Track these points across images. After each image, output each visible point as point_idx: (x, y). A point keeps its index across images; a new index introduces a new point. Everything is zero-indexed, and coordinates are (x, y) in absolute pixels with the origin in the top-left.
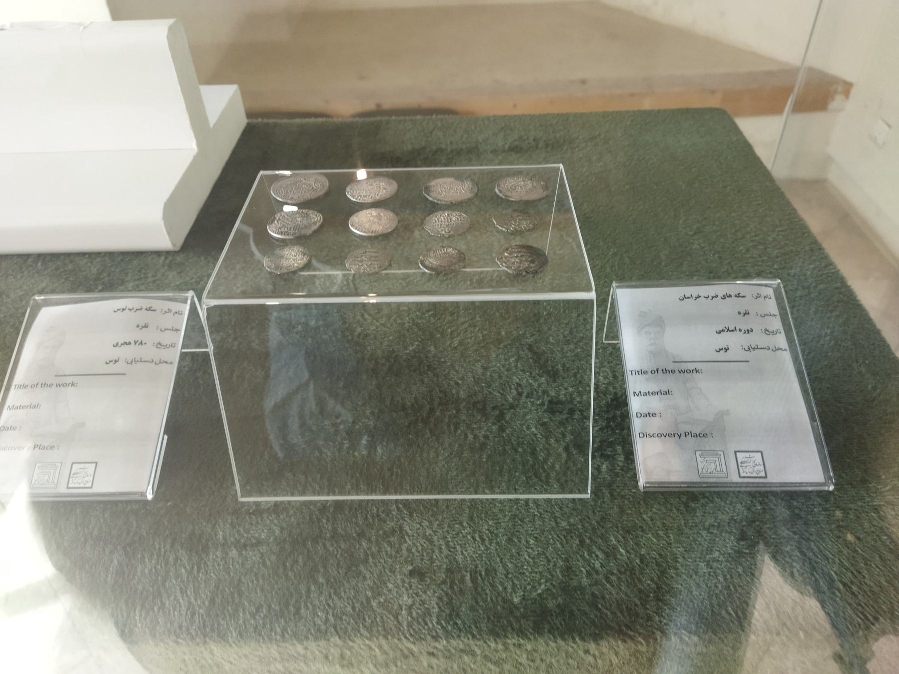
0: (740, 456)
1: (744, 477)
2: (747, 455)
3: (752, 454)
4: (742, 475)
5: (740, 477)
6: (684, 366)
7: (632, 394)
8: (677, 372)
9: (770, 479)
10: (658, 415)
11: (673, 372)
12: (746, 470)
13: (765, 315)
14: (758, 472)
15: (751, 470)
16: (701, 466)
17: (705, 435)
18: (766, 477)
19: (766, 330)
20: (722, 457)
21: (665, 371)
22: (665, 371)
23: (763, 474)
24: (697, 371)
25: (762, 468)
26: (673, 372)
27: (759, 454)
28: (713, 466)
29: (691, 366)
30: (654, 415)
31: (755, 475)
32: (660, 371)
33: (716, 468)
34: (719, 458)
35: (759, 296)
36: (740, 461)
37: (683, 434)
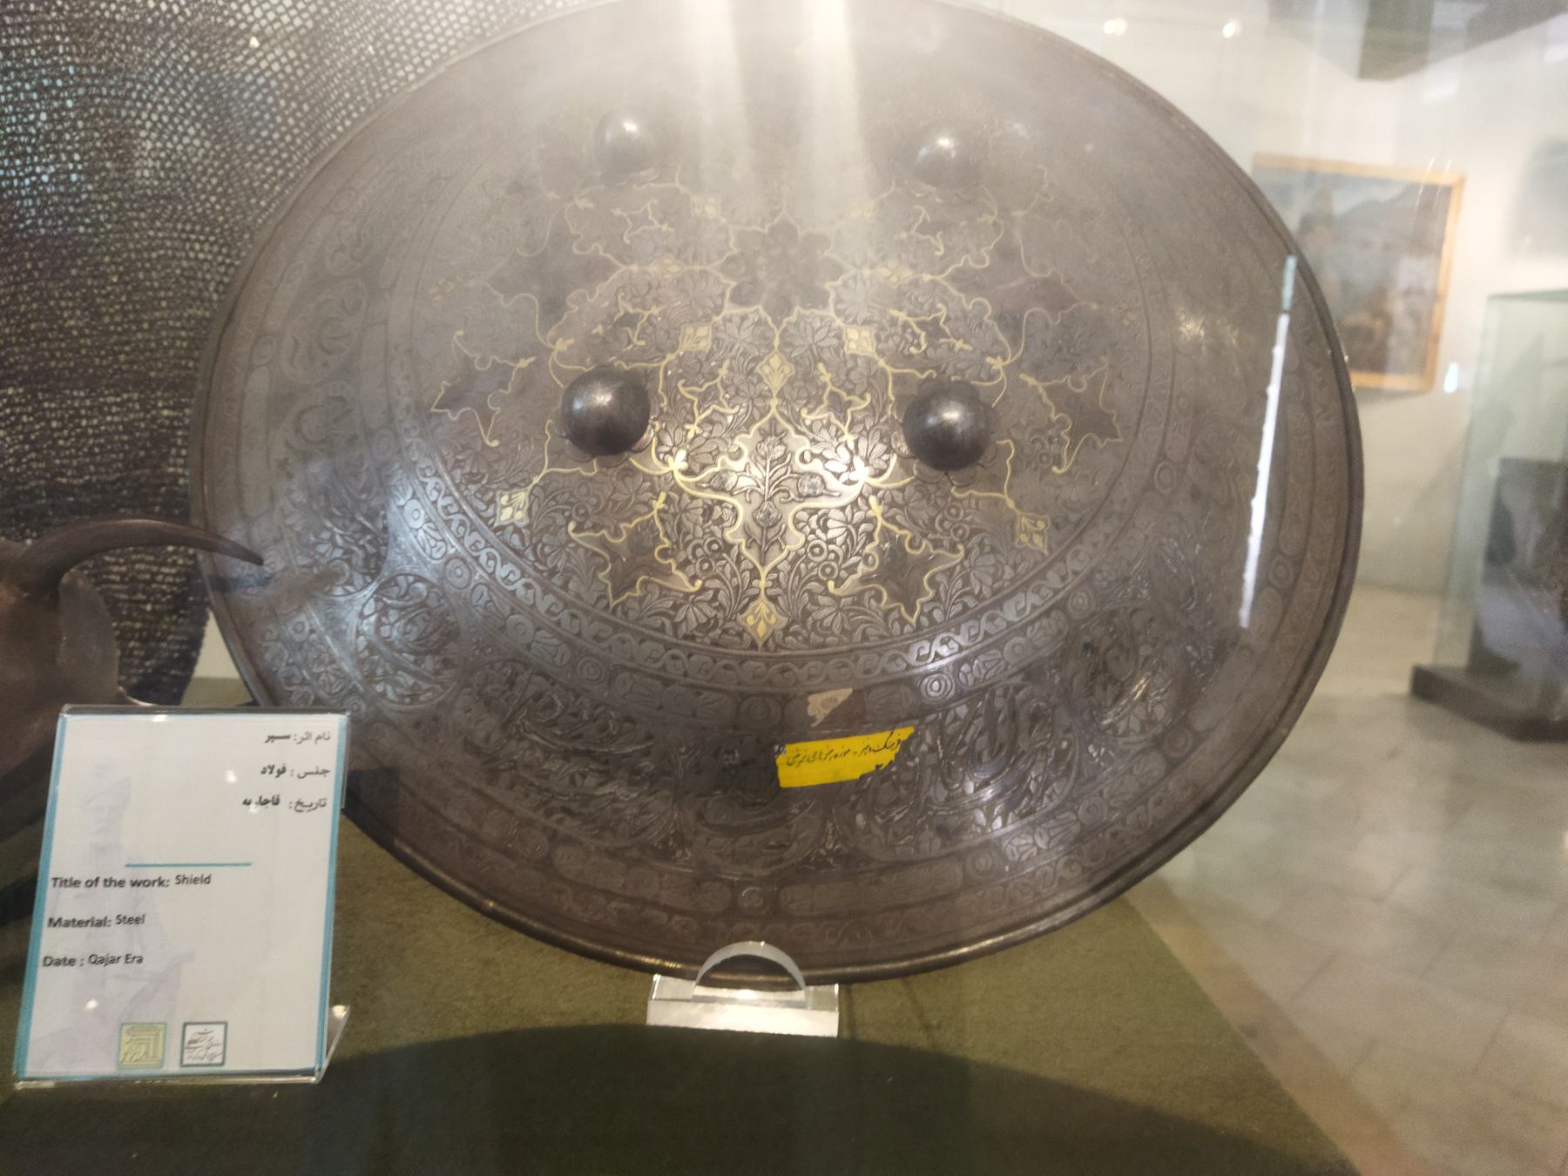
2: (201, 1028)
3: (210, 1028)
5: (182, 1065)
6: (142, 875)
7: (46, 922)
8: (128, 885)
9: (229, 1067)
10: (78, 963)
11: (121, 883)
14: (214, 1056)
16: (125, 1048)
18: (222, 1064)
19: (299, 803)
21: (109, 882)
22: (109, 882)
23: (218, 1060)
25: (220, 1049)
26: (121, 883)
27: (222, 1027)
28: (143, 1049)
29: (152, 874)
30: (72, 962)
31: (205, 1061)
32: (101, 883)
35: (308, 736)
36: (188, 1038)
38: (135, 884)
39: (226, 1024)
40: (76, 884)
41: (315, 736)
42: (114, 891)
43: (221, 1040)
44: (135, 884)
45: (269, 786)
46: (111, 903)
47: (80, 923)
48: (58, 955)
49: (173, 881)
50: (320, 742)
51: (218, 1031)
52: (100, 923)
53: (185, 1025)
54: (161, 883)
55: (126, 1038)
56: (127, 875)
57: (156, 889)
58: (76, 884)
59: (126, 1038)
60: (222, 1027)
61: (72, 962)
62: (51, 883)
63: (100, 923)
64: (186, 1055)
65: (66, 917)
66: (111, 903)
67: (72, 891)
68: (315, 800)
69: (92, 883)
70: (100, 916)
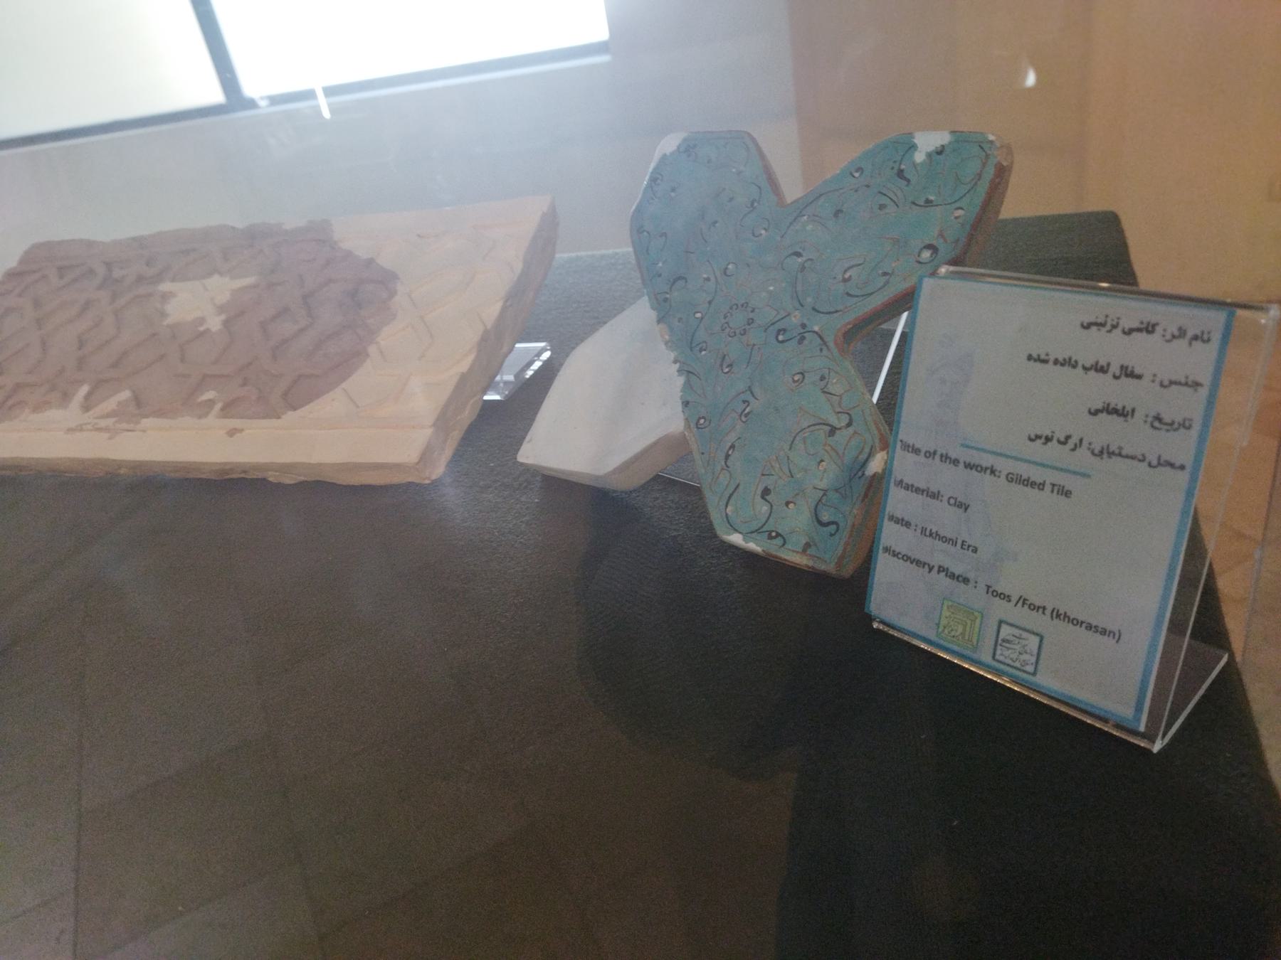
0: (1006, 631)
1: (999, 661)
2: (1017, 632)
3: (1025, 635)
4: (997, 657)
8: (961, 465)
11: (955, 462)
12: (1007, 653)
13: (1172, 383)
14: (1025, 663)
15: (1014, 656)
16: (944, 622)
17: (966, 581)
18: (1034, 674)
19: (1158, 418)
20: (978, 621)
21: (945, 458)
22: (945, 458)
23: (1030, 669)
24: (993, 472)
25: (1033, 660)
26: (955, 462)
27: (1037, 639)
28: (960, 629)
29: (987, 460)
30: (908, 525)
31: (1017, 664)
32: (937, 457)
33: (963, 634)
34: (973, 621)
35: (1182, 333)
37: (936, 569)
38: (969, 466)
40: (916, 451)
41: (1190, 334)
42: (947, 467)
43: (1035, 652)
44: (969, 466)
46: (948, 479)
47: (918, 490)
48: (899, 515)
50: (1198, 345)
51: (1034, 641)
52: (935, 496)
54: (993, 472)
55: (946, 613)
57: (988, 477)
58: (916, 451)
59: (946, 613)
61: (908, 525)
63: (935, 496)
64: (998, 652)
66: (948, 479)
67: (911, 457)
68: (1179, 419)
69: (931, 454)
70: (934, 489)
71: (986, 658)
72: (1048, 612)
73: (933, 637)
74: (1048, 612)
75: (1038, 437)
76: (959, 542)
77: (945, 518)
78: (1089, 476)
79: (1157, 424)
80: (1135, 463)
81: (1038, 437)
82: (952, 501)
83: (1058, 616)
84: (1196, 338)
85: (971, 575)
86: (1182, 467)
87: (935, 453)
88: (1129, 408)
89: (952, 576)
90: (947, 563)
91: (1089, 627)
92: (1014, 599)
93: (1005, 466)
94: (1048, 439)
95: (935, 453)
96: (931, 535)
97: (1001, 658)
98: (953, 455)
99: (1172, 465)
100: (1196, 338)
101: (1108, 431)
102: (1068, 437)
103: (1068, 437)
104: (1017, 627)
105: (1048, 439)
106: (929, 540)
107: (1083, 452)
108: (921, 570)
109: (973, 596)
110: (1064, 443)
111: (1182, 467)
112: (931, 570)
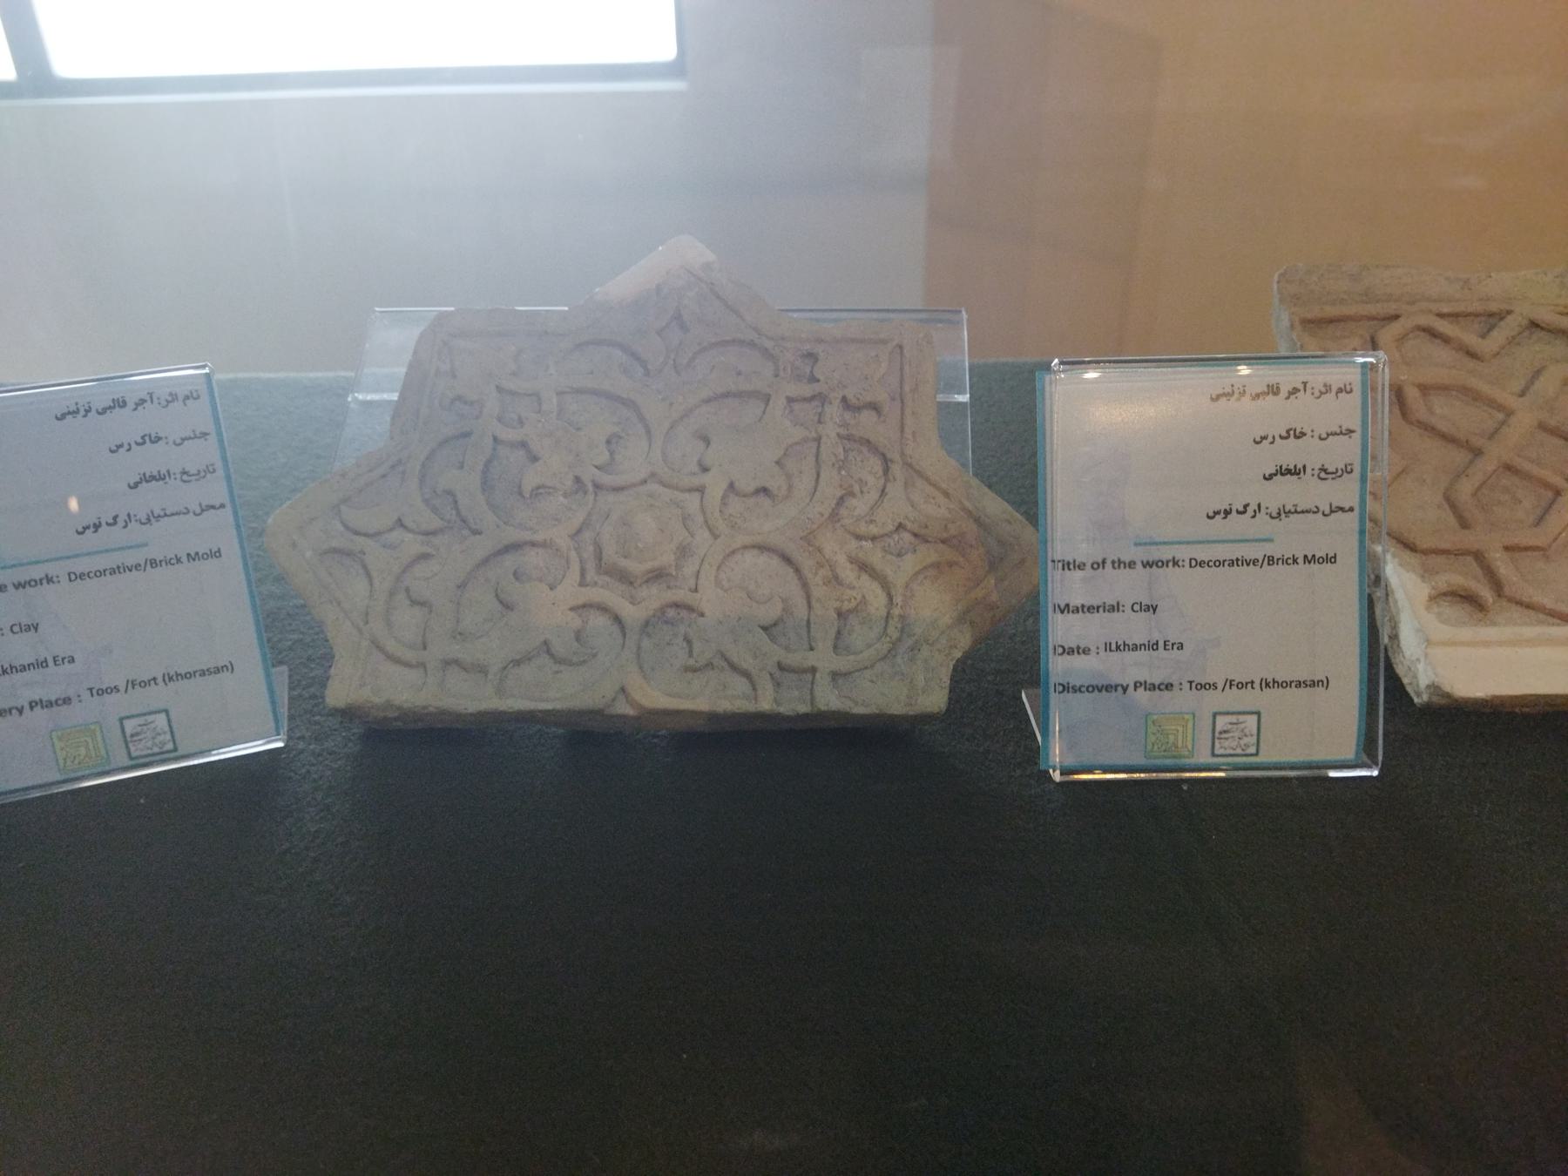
0: (1222, 722)
2: (1233, 719)
3: (1242, 718)
5: (1213, 755)
8: (1139, 566)
11: (1132, 565)
12: (1226, 744)
14: (1247, 746)
15: (1234, 744)
17: (1169, 687)
20: (1190, 725)
23: (1252, 750)
24: (1175, 563)
25: (1254, 740)
26: (1132, 565)
27: (1255, 717)
29: (1166, 553)
31: (1239, 751)
32: (1108, 565)
36: (1218, 728)
39: (1258, 714)
40: (1081, 567)
41: (1334, 389)
43: (1255, 731)
45: (1289, 453)
46: (1126, 586)
47: (1091, 609)
49: (1187, 563)
51: (1251, 721)
52: (1115, 608)
53: (1215, 715)
54: (1175, 563)
56: (1139, 554)
60: (1255, 717)
62: (1050, 564)
63: (1115, 608)
64: (1217, 745)
65: (1077, 601)
66: (1126, 586)
67: (1078, 574)
69: (1099, 565)
70: (1111, 601)
71: (1204, 758)
72: (1257, 685)
73: (1139, 760)
74: (1257, 685)
75: (1218, 513)
76: (1161, 644)
77: (1136, 628)
78: (1271, 540)
79: (1323, 475)
80: (1310, 515)
81: (1218, 513)
82: (1137, 607)
83: (1267, 685)
84: (1340, 390)
85: (1174, 680)
86: (1351, 509)
87: (1104, 562)
88: (1300, 466)
89: (1153, 687)
90: (1143, 675)
91: (1299, 684)
92: (1220, 687)
93: (1183, 553)
94: (1227, 513)
95: (1104, 562)
96: (1118, 648)
97: (1221, 751)
98: (1127, 559)
99: (1342, 509)
100: (1340, 390)
101: (1287, 492)
102: (1246, 506)
103: (1246, 506)
104: (1233, 713)
105: (1227, 513)
106: (1115, 656)
107: (1262, 516)
108: (1114, 694)
109: (1182, 700)
110: (1244, 512)
111: (1351, 509)
112: (1125, 690)
